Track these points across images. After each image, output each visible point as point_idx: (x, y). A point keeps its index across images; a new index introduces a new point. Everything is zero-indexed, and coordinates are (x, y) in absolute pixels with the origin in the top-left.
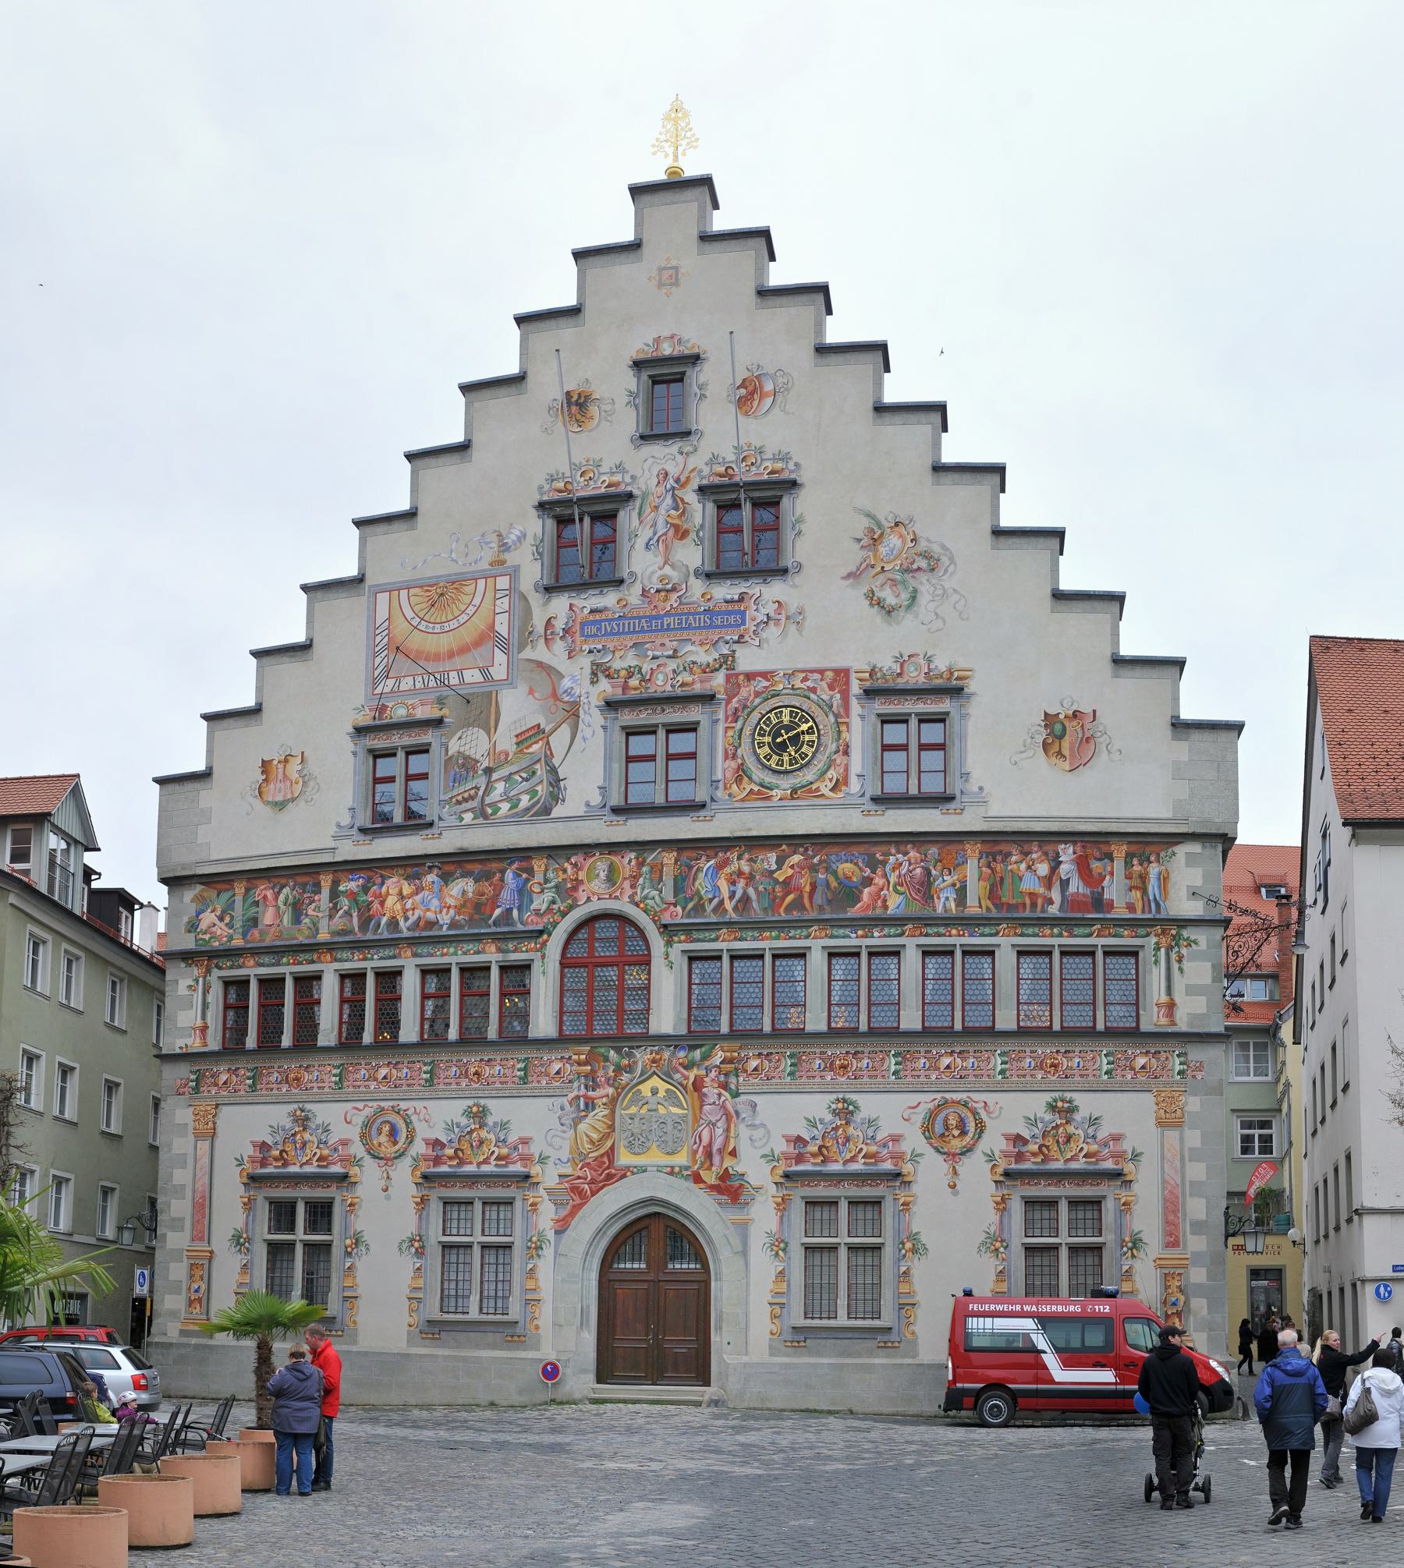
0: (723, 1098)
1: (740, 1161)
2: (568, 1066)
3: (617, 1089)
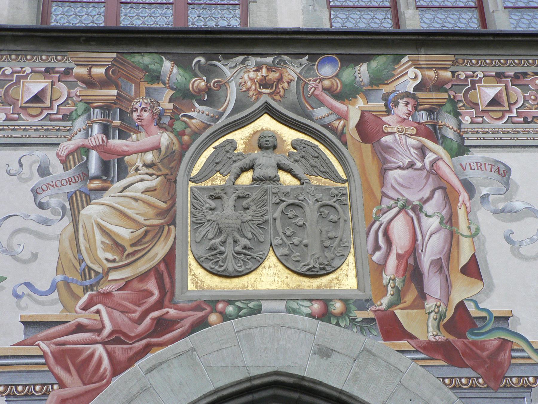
0: (430, 157)
1: (491, 288)
2: (62, 88)
3: (180, 135)
